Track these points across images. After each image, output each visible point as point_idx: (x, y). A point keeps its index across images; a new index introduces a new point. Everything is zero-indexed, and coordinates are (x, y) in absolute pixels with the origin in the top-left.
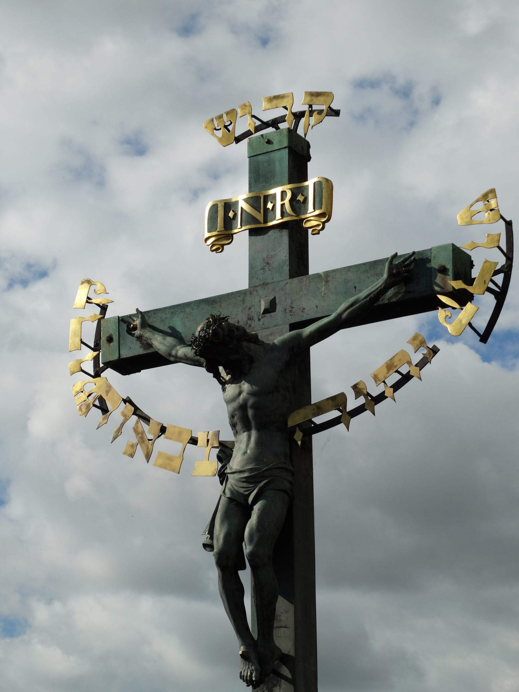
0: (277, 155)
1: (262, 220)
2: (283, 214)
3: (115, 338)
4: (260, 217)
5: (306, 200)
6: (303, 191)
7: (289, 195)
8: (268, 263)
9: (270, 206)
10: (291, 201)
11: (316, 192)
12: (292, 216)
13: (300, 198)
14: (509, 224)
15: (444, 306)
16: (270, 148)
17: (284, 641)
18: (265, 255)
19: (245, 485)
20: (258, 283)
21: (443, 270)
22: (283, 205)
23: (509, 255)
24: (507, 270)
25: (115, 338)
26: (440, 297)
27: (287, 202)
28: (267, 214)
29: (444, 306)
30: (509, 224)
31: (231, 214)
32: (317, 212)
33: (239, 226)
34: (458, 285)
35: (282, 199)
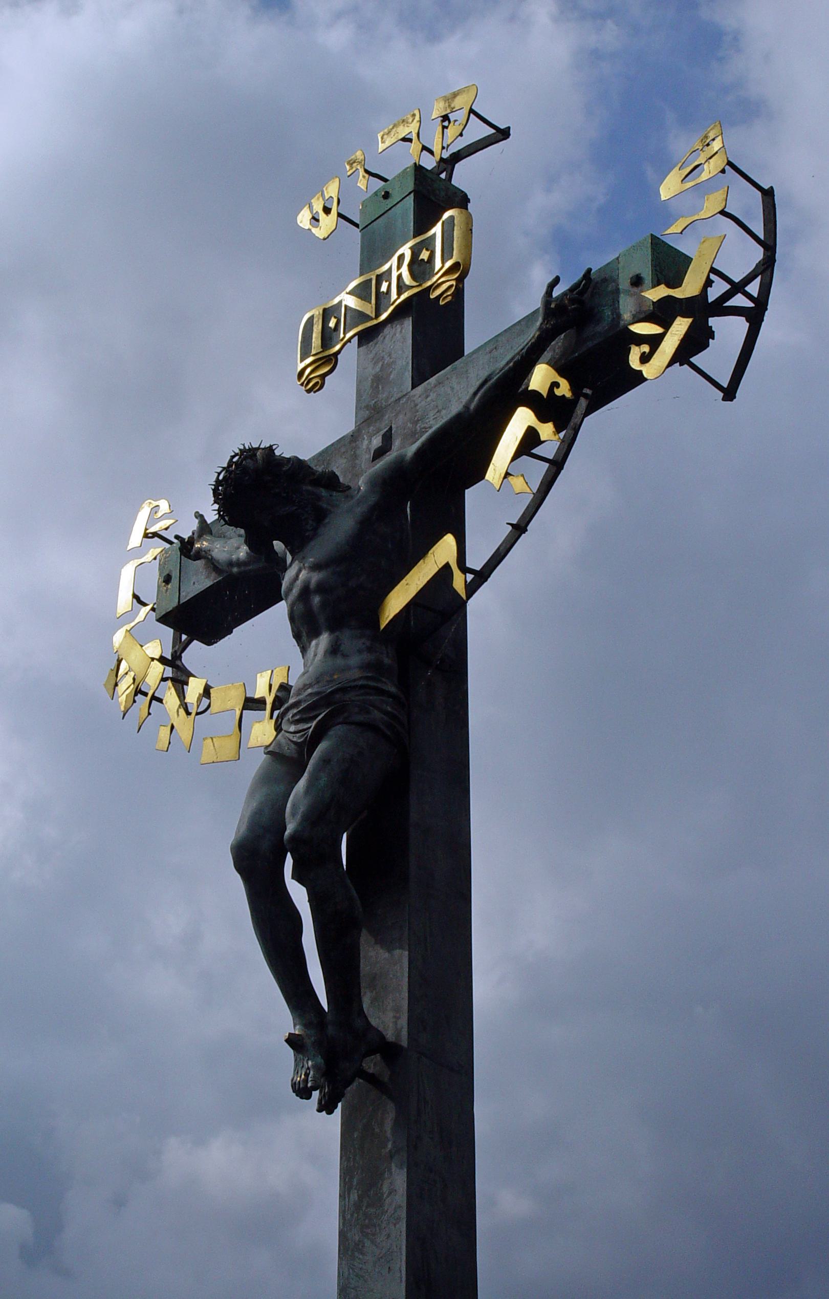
2: (401, 288)
3: (175, 575)
4: (369, 309)
6: (428, 244)
9: (384, 288)
11: (445, 235)
12: (413, 287)
14: (768, 195)
17: (389, 1013)
21: (637, 281)
22: (400, 277)
23: (769, 245)
24: (766, 268)
25: (175, 575)
27: (405, 271)
28: (381, 299)
29: (640, 339)
30: (768, 195)
31: (332, 324)
32: (449, 264)
35: (399, 268)
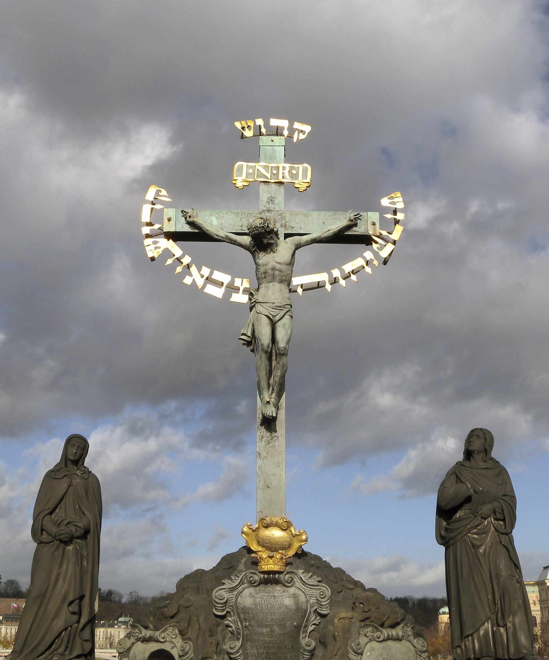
0: (278, 148)
1: (269, 178)
2: (283, 178)
4: (269, 176)
5: (297, 173)
7: (288, 169)
8: (271, 200)
10: (289, 172)
13: (294, 172)
15: (376, 242)
16: (273, 144)
18: (270, 195)
19: (274, 310)
20: (265, 209)
26: (373, 237)
27: (286, 172)
33: (256, 178)
34: (384, 233)
